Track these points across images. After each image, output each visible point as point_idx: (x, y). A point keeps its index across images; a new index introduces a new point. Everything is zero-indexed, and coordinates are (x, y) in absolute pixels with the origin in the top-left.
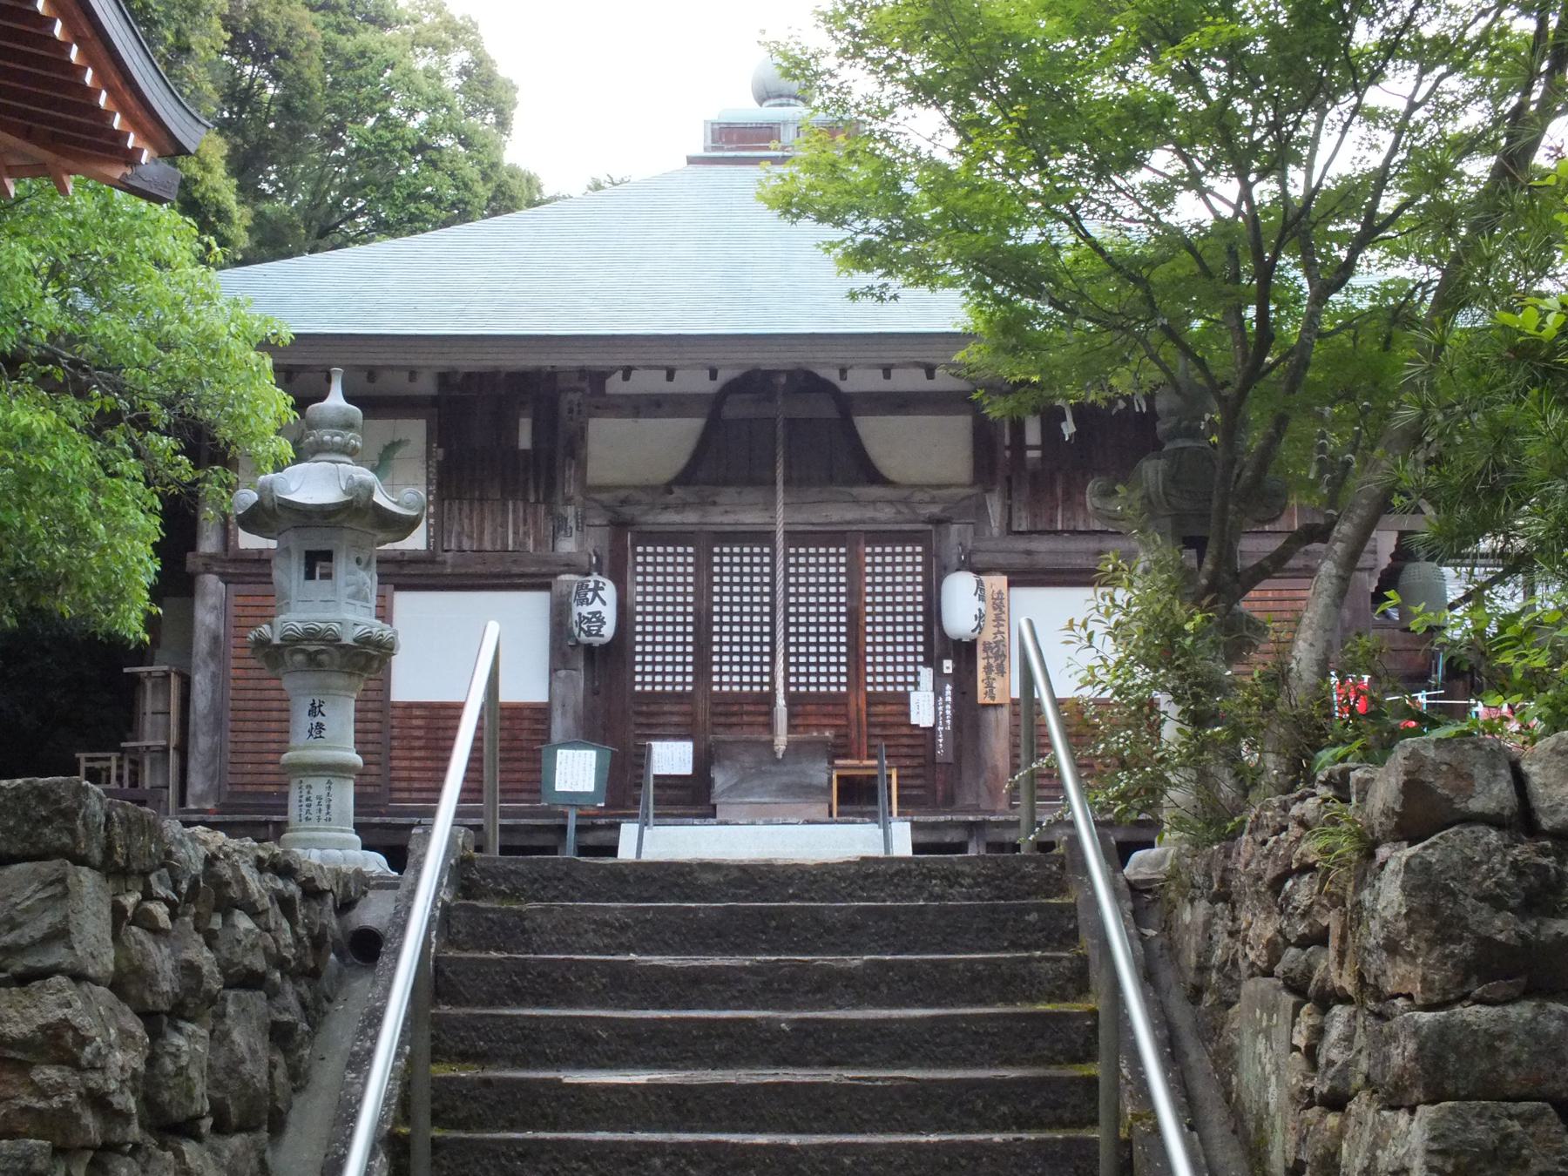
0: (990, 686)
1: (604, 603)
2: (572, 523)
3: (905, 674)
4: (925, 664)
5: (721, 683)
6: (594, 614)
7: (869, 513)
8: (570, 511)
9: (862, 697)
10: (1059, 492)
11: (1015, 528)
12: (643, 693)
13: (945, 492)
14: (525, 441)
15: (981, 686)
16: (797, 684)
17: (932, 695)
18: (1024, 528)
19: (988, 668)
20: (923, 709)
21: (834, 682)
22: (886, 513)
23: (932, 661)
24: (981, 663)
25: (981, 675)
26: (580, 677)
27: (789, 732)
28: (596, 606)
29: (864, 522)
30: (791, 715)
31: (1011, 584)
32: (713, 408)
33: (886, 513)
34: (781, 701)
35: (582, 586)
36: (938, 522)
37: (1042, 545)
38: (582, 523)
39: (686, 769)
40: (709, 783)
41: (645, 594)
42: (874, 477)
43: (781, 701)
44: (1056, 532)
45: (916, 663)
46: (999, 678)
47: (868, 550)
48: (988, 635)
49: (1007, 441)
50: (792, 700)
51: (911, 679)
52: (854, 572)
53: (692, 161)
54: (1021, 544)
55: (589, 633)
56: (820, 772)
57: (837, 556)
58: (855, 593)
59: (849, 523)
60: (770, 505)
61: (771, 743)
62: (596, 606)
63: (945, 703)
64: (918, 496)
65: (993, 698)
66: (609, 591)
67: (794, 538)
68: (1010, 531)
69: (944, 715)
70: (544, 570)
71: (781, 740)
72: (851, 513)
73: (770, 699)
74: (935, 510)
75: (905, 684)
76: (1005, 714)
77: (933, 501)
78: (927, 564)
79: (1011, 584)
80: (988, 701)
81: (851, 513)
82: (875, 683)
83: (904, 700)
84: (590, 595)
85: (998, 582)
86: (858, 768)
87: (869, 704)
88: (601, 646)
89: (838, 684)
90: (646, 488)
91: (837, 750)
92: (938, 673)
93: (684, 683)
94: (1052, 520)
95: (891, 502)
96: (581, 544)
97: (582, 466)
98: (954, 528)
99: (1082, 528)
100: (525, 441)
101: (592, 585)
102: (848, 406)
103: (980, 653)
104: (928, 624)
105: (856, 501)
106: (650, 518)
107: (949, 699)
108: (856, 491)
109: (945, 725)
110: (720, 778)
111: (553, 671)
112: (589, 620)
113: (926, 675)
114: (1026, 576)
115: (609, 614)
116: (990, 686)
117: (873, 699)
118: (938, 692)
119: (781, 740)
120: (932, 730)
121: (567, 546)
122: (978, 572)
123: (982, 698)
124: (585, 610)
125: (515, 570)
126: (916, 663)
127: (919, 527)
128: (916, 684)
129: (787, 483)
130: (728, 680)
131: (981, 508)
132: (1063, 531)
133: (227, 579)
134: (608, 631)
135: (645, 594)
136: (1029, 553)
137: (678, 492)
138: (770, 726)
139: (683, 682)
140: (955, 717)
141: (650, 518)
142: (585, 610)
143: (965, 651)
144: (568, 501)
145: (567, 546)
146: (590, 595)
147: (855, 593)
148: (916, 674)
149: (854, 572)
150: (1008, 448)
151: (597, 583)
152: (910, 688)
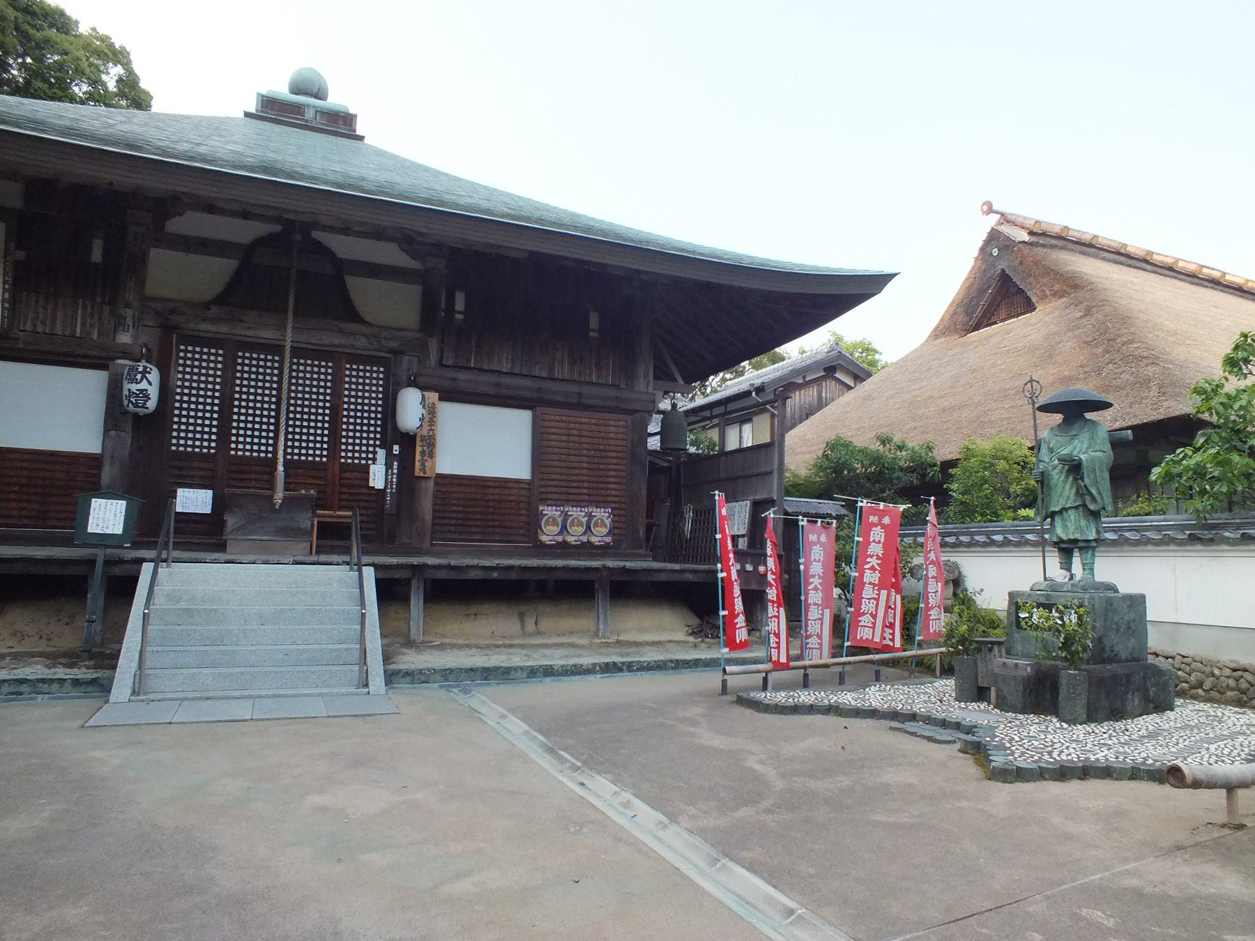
0: (423, 465)
1: (150, 384)
2: (129, 321)
3: (367, 452)
4: (381, 447)
5: (237, 449)
6: (141, 391)
7: (350, 341)
8: (129, 313)
9: (337, 468)
11: (444, 363)
12: (177, 452)
13: (402, 334)
14: (97, 255)
15: (417, 464)
16: (293, 454)
17: (384, 467)
18: (450, 363)
19: (423, 453)
20: (378, 477)
21: (320, 454)
22: (362, 342)
24: (418, 449)
25: (418, 457)
26: (127, 438)
27: (286, 490)
28: (144, 385)
29: (346, 347)
30: (287, 476)
31: (441, 399)
32: (247, 254)
33: (362, 342)
34: (280, 468)
35: (133, 370)
36: (397, 352)
37: (462, 376)
39: (208, 510)
40: (222, 524)
41: (183, 380)
42: (356, 317)
43: (280, 468)
44: (469, 368)
45: (375, 446)
46: (429, 460)
47: (348, 366)
48: (425, 432)
49: (443, 307)
50: (287, 464)
51: (371, 456)
52: (337, 380)
53: (247, 115)
54: (449, 374)
55: (136, 405)
56: (306, 520)
57: (327, 368)
58: (337, 393)
59: (337, 346)
60: (282, 327)
61: (271, 497)
62: (144, 385)
63: (393, 474)
64: (384, 334)
65: (425, 473)
66: (154, 375)
67: (298, 352)
68: (441, 364)
69: (392, 481)
70: (103, 354)
71: (279, 496)
72: (338, 340)
74: (394, 344)
75: (367, 459)
76: (431, 484)
78: (386, 379)
79: (441, 399)
80: (421, 474)
81: (338, 340)
82: (346, 457)
83: (365, 470)
84: (139, 377)
85: (433, 396)
86: (331, 517)
87: (341, 471)
88: (145, 415)
89: (321, 456)
91: (320, 503)
92: (389, 454)
93: (209, 448)
94: (468, 360)
95: (366, 336)
96: (135, 338)
97: (142, 282)
99: (486, 368)
100: (97, 255)
101: (141, 369)
102: (342, 267)
103: (418, 443)
104: (384, 420)
105: (342, 332)
106: (191, 325)
107: (395, 471)
108: (343, 325)
109: (392, 488)
110: (231, 521)
111: (106, 430)
112: (137, 395)
113: (381, 454)
114: (450, 395)
115: (154, 392)
116: (423, 465)
117: (345, 468)
118: (388, 466)
119: (279, 496)
120: (383, 492)
121: (125, 338)
122: (422, 388)
123: (418, 473)
124: (134, 387)
125: (80, 352)
126: (375, 446)
127: (383, 354)
128: (374, 460)
129: (295, 314)
130: (241, 447)
131: (424, 348)
132: (474, 368)
134: (152, 404)
135: (183, 380)
136: (454, 379)
137: (215, 310)
138: (271, 486)
139: (206, 444)
140: (398, 483)
141: (191, 325)
142: (134, 387)
143: (408, 440)
144: (128, 305)
145: (125, 338)
146: (139, 377)
147: (337, 393)
148: (375, 453)
149: (337, 380)
151: (145, 368)
152: (370, 462)
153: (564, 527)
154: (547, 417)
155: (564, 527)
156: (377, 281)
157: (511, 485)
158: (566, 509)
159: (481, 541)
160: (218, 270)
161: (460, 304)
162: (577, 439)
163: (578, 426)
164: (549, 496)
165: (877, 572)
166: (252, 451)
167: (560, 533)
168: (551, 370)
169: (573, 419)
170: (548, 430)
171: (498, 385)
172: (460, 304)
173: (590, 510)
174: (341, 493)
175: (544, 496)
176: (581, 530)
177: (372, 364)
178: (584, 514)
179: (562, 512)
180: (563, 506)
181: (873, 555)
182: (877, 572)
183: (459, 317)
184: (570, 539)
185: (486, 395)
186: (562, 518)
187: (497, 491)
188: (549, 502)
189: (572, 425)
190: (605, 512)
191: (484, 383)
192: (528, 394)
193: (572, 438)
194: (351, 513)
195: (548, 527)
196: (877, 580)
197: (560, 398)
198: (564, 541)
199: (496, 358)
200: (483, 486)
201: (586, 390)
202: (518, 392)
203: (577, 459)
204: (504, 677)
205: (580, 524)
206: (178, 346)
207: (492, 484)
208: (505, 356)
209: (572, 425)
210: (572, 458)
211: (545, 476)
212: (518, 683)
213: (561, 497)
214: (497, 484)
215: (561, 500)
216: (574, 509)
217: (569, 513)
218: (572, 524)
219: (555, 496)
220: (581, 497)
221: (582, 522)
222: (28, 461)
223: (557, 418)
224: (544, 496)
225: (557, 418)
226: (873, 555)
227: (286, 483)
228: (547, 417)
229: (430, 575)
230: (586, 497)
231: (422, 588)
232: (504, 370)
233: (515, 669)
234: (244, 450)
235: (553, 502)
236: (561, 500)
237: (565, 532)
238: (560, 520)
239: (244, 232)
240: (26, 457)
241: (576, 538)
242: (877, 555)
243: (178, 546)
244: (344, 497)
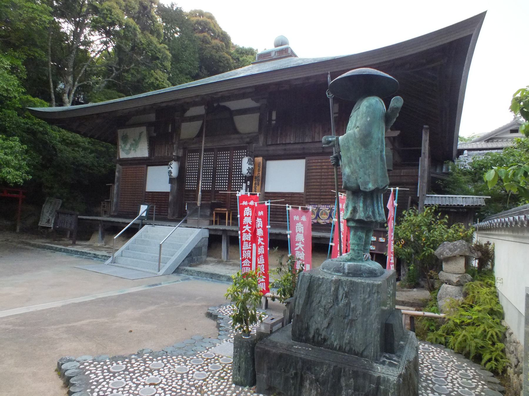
1: (172, 168)
2: (175, 149)
3: (240, 185)
4: (245, 183)
5: (187, 187)
10: (279, 133)
12: (187, 190)
13: (251, 135)
16: (204, 188)
18: (270, 143)
19: (255, 184)
23: (246, 182)
27: (202, 201)
30: (202, 195)
33: (236, 142)
34: (200, 193)
38: (178, 148)
43: (200, 193)
44: (277, 144)
46: (258, 186)
49: (268, 120)
50: (202, 191)
52: (231, 158)
57: (227, 154)
61: (196, 204)
71: (199, 203)
73: (196, 191)
74: (248, 140)
77: (248, 137)
86: (220, 211)
90: (190, 139)
92: (247, 186)
94: (277, 141)
98: (254, 145)
99: (284, 143)
102: (232, 113)
103: (254, 180)
113: (244, 185)
119: (199, 203)
127: (245, 145)
128: (242, 188)
129: (206, 136)
133: (121, 165)
136: (267, 151)
148: (242, 185)
149: (231, 158)
150: (268, 121)
153: (318, 215)
154: (311, 161)
155: (318, 215)
156: (245, 115)
157: (296, 195)
158: (332, 206)
159: (282, 221)
160: (196, 125)
161: (274, 117)
162: (326, 170)
163: (326, 164)
164: (311, 200)
165: (249, 234)
166: (189, 188)
167: (316, 218)
168: (313, 138)
169: (324, 160)
170: (312, 168)
171: (285, 150)
172: (274, 117)
173: (332, 206)
174: (231, 201)
175: (309, 200)
176: (326, 217)
177: (238, 150)
178: (328, 208)
179: (317, 208)
180: (317, 205)
181: (246, 224)
182: (249, 234)
183: (274, 122)
184: (321, 221)
185: (297, 154)
186: (317, 211)
187: (290, 198)
188: (311, 203)
189: (324, 164)
190: (327, 207)
191: (279, 150)
192: (298, 152)
193: (323, 170)
194: (226, 209)
195: (322, 216)
196: (250, 238)
197: (314, 151)
198: (318, 223)
199: (288, 137)
200: (284, 197)
201: (307, 146)
202: (294, 152)
203: (326, 180)
204: (219, 278)
205: (326, 214)
206: (188, 154)
207: (287, 195)
208: (292, 135)
209: (324, 164)
210: (323, 180)
211: (310, 190)
212: (223, 283)
213: (317, 200)
214: (290, 195)
215: (317, 202)
216: (323, 206)
217: (320, 208)
218: (322, 214)
219: (314, 200)
220: (327, 200)
221: (327, 213)
222: (158, 195)
223: (316, 161)
224: (309, 200)
225: (316, 161)
226: (246, 224)
227: (202, 198)
228: (311, 161)
229: (229, 234)
230: (330, 200)
231: (225, 238)
232: (292, 142)
233: (223, 276)
234: (208, 188)
235: (313, 203)
236: (317, 202)
237: (318, 218)
238: (315, 212)
239: (200, 110)
240: (157, 194)
241: (324, 221)
242: (249, 224)
243: (157, 219)
244: (232, 203)
